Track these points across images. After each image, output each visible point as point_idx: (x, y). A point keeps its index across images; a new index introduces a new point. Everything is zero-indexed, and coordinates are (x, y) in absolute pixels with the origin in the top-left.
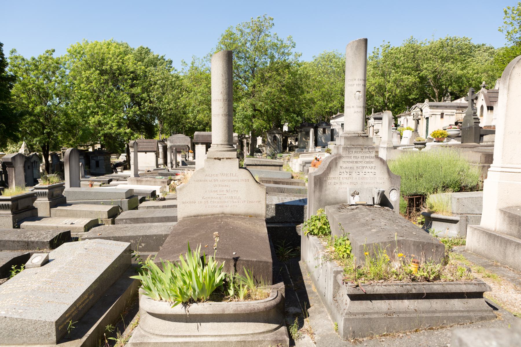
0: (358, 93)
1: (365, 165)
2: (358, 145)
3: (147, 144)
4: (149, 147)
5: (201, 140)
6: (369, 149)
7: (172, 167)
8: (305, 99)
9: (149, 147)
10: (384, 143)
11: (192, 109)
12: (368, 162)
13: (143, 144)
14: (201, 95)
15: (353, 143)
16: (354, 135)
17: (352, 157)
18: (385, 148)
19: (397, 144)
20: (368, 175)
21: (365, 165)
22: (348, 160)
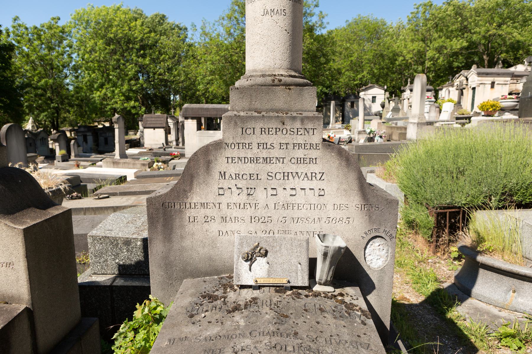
1: (293, 168)
2: (272, 110)
3: (156, 119)
4: (158, 122)
5: (191, 114)
6: (302, 120)
7: (177, 145)
8: (330, 69)
9: (158, 122)
10: (414, 117)
11: (201, 79)
12: (299, 161)
13: (151, 119)
15: (257, 105)
16: (260, 80)
17: (255, 146)
18: (415, 123)
19: (436, 120)
20: (300, 198)
21: (293, 168)
22: (242, 155)
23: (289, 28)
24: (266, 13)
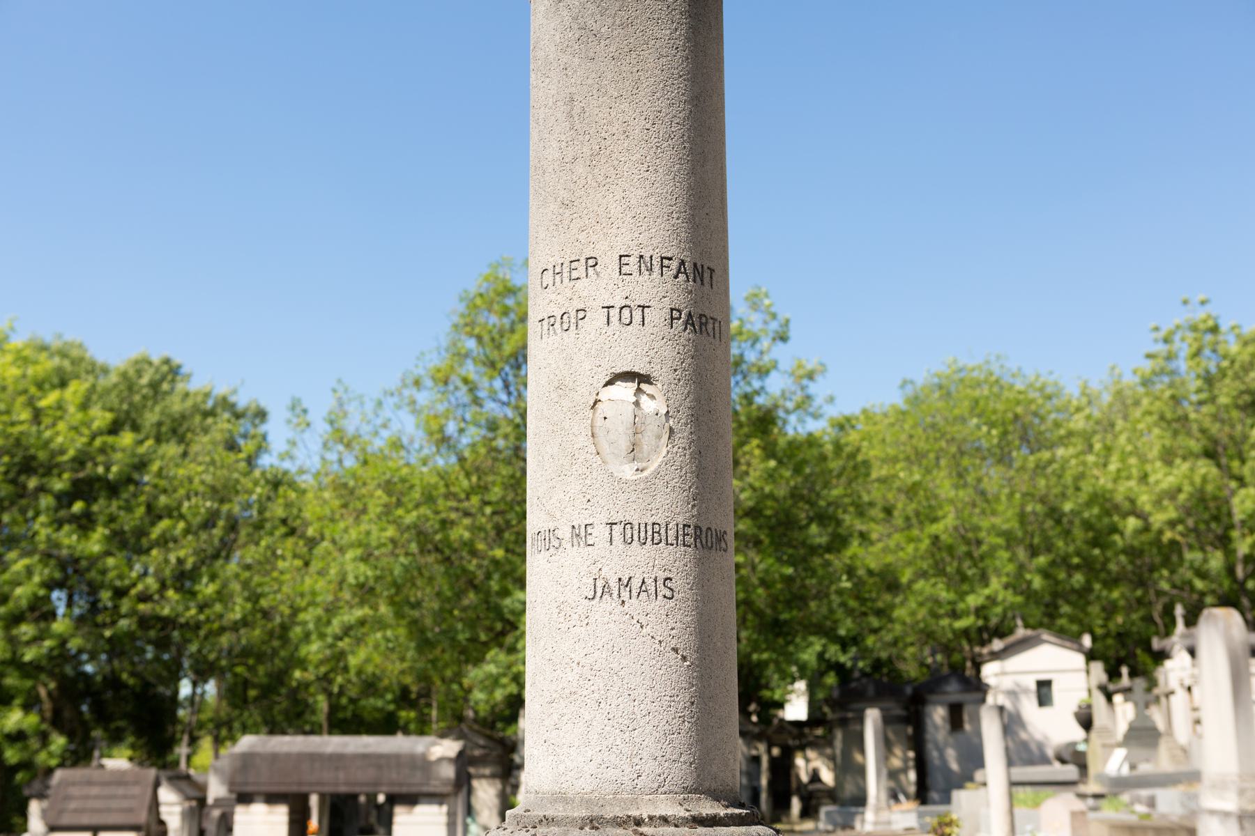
0: (625, 391)
4: (114, 804)
5: (263, 779)
8: (851, 572)
11: (318, 620)
14: (365, 559)
18: (1226, 814)
23: (686, 642)
24: (601, 591)
